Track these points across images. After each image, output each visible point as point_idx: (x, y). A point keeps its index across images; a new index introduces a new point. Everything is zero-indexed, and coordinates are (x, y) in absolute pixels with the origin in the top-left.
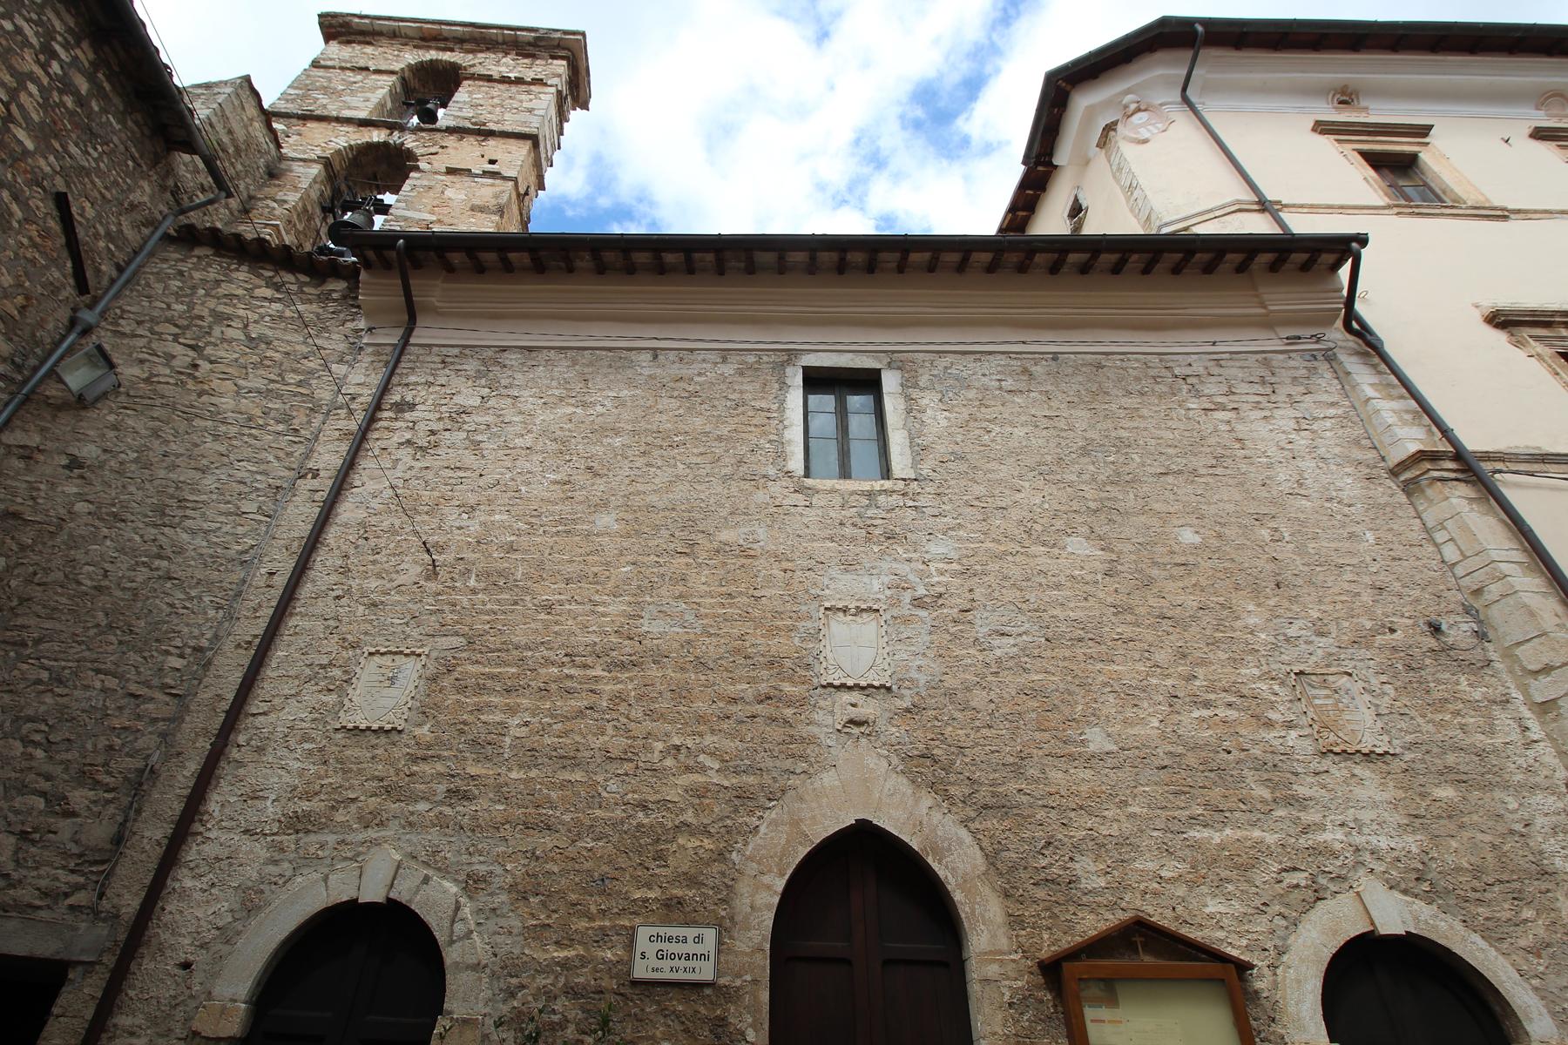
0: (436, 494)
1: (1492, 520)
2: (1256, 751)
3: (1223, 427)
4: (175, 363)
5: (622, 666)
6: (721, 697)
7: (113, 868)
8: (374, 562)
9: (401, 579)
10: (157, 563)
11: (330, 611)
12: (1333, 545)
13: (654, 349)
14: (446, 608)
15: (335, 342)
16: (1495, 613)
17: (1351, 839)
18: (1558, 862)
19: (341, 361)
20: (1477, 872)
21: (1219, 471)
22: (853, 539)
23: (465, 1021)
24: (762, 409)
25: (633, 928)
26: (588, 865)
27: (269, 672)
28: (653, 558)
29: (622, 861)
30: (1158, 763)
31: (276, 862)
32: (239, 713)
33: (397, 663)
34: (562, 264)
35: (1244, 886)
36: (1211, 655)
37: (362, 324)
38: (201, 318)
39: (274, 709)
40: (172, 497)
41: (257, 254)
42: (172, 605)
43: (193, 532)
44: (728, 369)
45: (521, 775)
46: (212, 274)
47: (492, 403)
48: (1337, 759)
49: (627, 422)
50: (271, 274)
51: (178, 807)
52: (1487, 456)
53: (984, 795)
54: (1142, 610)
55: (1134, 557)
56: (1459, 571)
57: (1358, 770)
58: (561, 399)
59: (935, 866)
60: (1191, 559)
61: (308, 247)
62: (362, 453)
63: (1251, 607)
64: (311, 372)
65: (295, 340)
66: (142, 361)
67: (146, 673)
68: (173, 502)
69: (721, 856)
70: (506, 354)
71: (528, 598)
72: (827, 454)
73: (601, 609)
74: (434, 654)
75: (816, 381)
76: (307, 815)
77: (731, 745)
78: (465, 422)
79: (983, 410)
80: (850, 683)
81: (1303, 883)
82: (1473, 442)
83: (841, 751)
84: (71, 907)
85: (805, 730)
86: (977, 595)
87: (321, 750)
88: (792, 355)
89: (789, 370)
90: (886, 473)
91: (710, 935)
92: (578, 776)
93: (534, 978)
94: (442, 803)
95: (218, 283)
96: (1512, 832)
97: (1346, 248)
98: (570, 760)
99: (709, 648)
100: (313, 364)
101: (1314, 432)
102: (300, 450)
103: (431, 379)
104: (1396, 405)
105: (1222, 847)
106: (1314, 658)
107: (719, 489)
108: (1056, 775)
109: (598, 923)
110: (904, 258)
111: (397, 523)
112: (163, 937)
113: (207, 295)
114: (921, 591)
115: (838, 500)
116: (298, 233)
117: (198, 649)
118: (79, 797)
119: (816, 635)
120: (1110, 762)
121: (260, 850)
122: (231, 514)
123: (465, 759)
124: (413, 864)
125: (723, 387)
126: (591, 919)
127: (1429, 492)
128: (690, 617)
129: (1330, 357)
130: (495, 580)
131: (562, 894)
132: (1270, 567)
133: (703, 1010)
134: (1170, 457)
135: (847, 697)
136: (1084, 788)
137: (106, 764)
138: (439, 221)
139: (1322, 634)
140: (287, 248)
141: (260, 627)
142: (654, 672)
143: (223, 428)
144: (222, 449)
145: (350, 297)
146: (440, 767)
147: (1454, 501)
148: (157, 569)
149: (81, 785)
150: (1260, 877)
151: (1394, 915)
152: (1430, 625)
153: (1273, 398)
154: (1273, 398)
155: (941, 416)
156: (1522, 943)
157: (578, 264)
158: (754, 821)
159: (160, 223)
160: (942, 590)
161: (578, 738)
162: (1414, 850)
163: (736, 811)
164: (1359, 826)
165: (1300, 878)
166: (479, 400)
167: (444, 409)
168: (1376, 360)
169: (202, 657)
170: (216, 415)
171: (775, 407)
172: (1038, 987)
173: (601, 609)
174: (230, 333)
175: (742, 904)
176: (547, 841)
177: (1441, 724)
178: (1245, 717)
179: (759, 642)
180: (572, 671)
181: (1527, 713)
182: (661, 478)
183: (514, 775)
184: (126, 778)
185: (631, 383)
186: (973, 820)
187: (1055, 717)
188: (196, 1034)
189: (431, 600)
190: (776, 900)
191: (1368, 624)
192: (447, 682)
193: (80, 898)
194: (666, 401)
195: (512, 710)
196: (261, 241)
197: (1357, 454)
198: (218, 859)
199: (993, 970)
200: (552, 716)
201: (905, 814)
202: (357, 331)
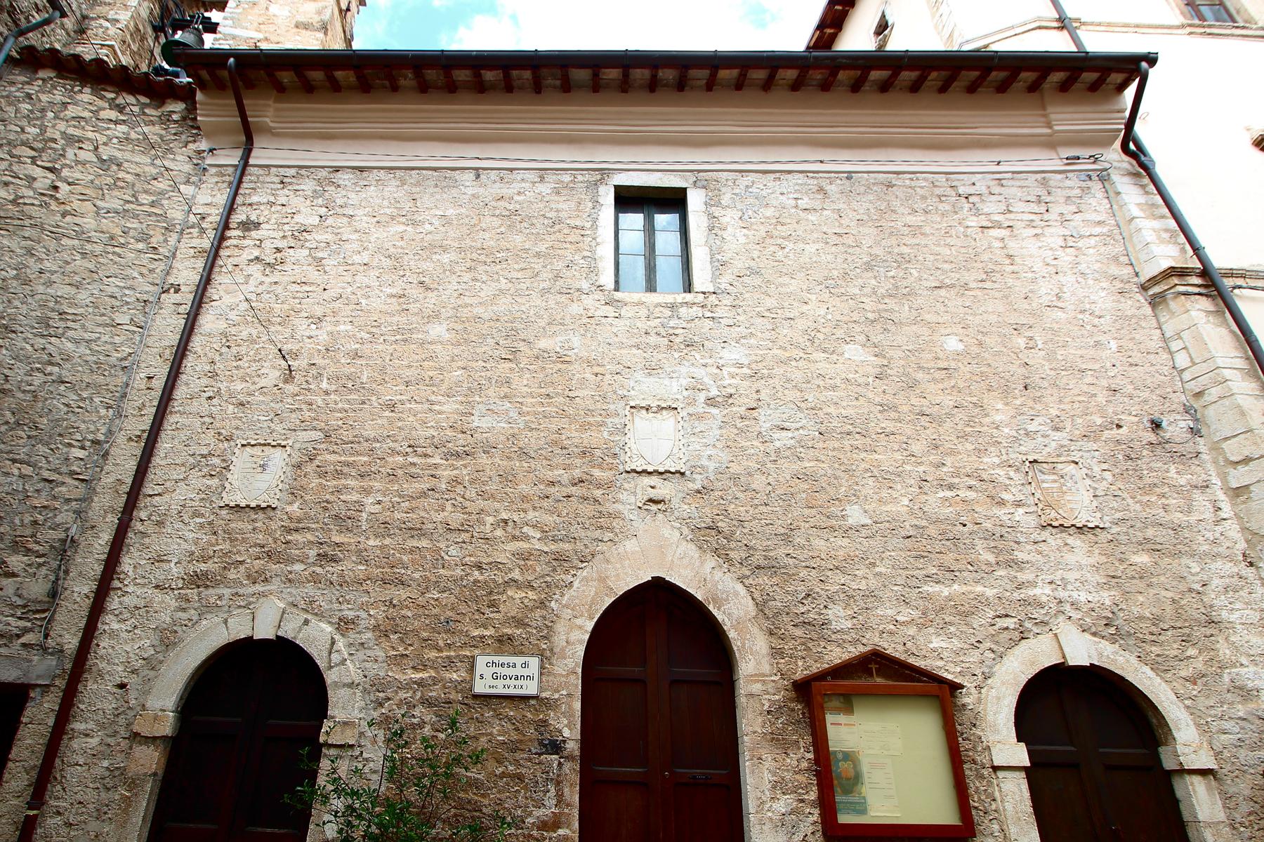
1: (1223, 331)
2: (988, 525)
3: (997, 244)
5: (458, 455)
7: (53, 616)
9: (263, 382)
10: (49, 369)
11: (205, 408)
12: (1079, 352)
13: (477, 169)
14: (303, 406)
15: (180, 163)
16: (1211, 413)
17: (1056, 594)
18: (1224, 614)
19: (188, 182)
20: (1156, 620)
21: (988, 285)
22: (656, 347)
23: (345, 723)
24: (576, 227)
25: (473, 657)
27: (156, 460)
29: (463, 608)
30: (904, 533)
32: (138, 494)
33: (266, 453)
34: (387, 83)
35: (964, 628)
37: (203, 145)
38: (54, 141)
39: (167, 491)
40: (53, 310)
42: (67, 405)
43: (76, 342)
44: (545, 189)
45: (378, 543)
46: (58, 96)
47: (330, 221)
48: (1054, 531)
49: (454, 239)
50: (113, 95)
51: (99, 569)
52: (1231, 274)
53: (758, 559)
54: (905, 409)
56: (1187, 376)
57: (1070, 540)
59: (715, 612)
60: (953, 365)
61: (144, 68)
62: (216, 269)
64: (162, 193)
66: (6, 184)
67: (55, 461)
68: (55, 315)
70: (339, 175)
71: (374, 398)
72: (635, 269)
74: (297, 446)
75: (628, 199)
76: (205, 574)
77: (550, 519)
78: (306, 240)
79: (779, 227)
80: (650, 469)
81: (1012, 626)
82: (1219, 259)
83: (640, 523)
85: (612, 508)
86: (763, 396)
87: (210, 523)
89: (602, 189)
90: (688, 287)
92: (424, 543)
93: (397, 692)
95: (65, 105)
96: (1190, 590)
97: (1133, 68)
98: (418, 531)
99: (531, 441)
100: (162, 185)
101: (1078, 249)
102: (160, 267)
103: (272, 199)
104: (1157, 224)
105: (949, 598)
107: (538, 302)
108: (819, 543)
109: (445, 654)
110: (713, 76)
111: (254, 333)
112: (101, 666)
114: (714, 392)
115: (643, 312)
116: (133, 53)
117: (96, 442)
119: (622, 430)
120: (864, 533)
121: (170, 601)
122: (107, 325)
123: (330, 530)
124: (294, 610)
125: (541, 205)
127: (1173, 305)
129: (1104, 177)
131: (416, 632)
132: (1022, 371)
134: (945, 272)
135: (647, 481)
138: (266, 39)
140: (125, 68)
141: (146, 423)
142: (484, 460)
144: (91, 266)
145: (189, 119)
146: (309, 537)
147: (1193, 313)
148: (50, 374)
149: (16, 552)
151: (1082, 651)
152: (1153, 422)
153: (1046, 217)
154: (1046, 217)
155: (740, 234)
156: (1183, 673)
157: (402, 82)
160: (733, 391)
161: (423, 514)
162: (1108, 602)
164: (1065, 583)
166: (318, 219)
167: (286, 227)
168: (1147, 180)
169: (100, 448)
170: (80, 234)
171: (588, 225)
173: (437, 407)
174: (83, 155)
177: (1148, 504)
178: (982, 498)
179: (574, 436)
180: (415, 460)
181: (1221, 496)
184: (52, 547)
185: (456, 202)
186: (748, 577)
187: (821, 498)
188: (137, 734)
191: (1099, 421)
192: (309, 468)
194: (488, 219)
195: (367, 491)
196: (99, 62)
197: (1114, 270)
200: (400, 496)
201: (692, 572)
202: (199, 152)
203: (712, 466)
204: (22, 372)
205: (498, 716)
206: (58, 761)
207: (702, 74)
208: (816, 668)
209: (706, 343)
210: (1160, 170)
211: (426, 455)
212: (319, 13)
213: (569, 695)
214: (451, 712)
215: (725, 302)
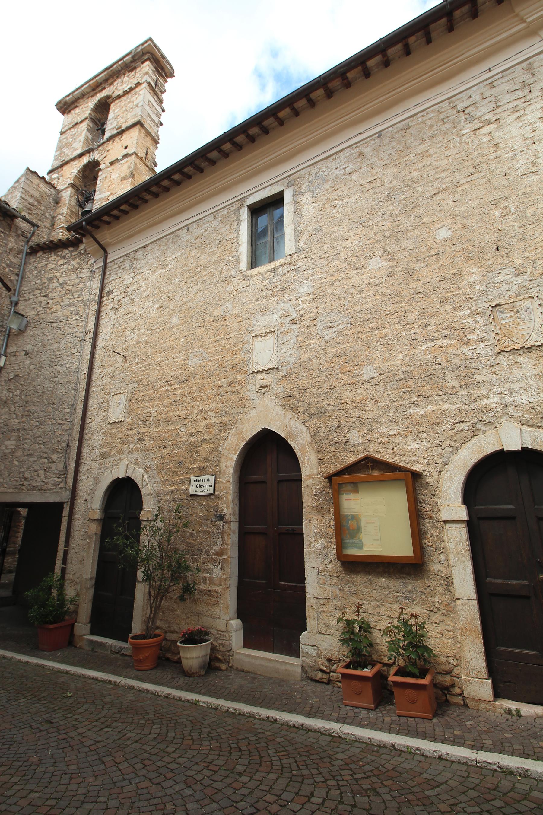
0: (123, 327)
2: (456, 361)
4: (43, 304)
6: (215, 387)
8: (110, 361)
26: (177, 458)
27: (90, 408)
28: (192, 332)
30: (398, 378)
31: (100, 469)
35: (432, 434)
36: (441, 309)
41: (53, 247)
42: (62, 393)
43: (62, 366)
48: (507, 355)
53: (313, 410)
55: (407, 259)
57: (520, 359)
58: (157, 267)
63: (475, 270)
65: (72, 279)
68: (54, 357)
69: (216, 449)
73: (175, 360)
77: (219, 406)
81: (466, 428)
84: (60, 488)
85: (244, 394)
88: (243, 200)
91: (212, 478)
92: (172, 427)
94: (136, 443)
98: (169, 422)
99: (211, 367)
106: (510, 293)
113: (45, 272)
117: (72, 405)
118: (54, 457)
120: (373, 383)
123: (141, 427)
126: (179, 476)
128: (204, 355)
130: (144, 357)
133: (211, 503)
135: (260, 376)
136: (359, 398)
137: (58, 446)
139: (520, 275)
143: (61, 324)
150: (440, 429)
158: (227, 435)
159: (23, 250)
163: (221, 432)
165: (465, 426)
172: (327, 487)
175: (223, 466)
176: (165, 452)
182: (193, 291)
183: (154, 430)
186: (308, 421)
189: (126, 371)
190: (234, 463)
193: (62, 485)
198: (88, 470)
199: (310, 482)
200: (164, 407)
201: (281, 423)
203: (291, 360)
204: (47, 383)
207: (320, 92)
211: (172, 385)
212: (129, 168)
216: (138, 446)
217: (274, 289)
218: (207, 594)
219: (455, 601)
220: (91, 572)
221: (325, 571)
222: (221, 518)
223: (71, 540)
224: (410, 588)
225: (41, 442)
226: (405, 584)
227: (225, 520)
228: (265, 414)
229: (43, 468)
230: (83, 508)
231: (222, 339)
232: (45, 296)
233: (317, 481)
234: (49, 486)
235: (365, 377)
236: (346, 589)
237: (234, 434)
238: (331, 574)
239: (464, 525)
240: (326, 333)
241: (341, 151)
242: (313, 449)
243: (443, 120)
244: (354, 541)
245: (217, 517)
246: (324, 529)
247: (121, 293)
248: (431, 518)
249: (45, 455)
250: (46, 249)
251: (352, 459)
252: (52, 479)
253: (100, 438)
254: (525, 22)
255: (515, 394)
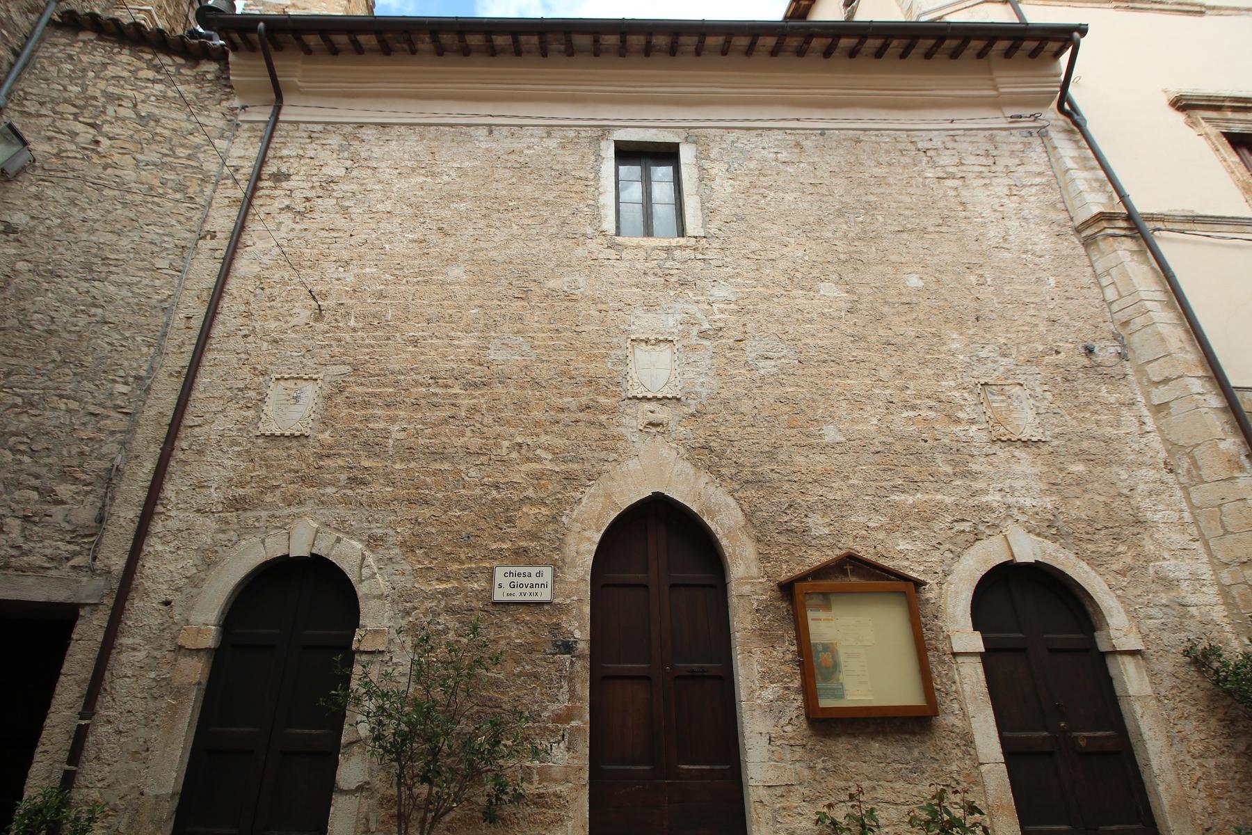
0: (316, 251)
1: (1145, 268)
2: (946, 441)
3: (952, 193)
4: (79, 139)
5: (476, 385)
6: (552, 408)
7: (100, 540)
8: (271, 308)
9: (294, 321)
10: (93, 310)
11: (240, 344)
12: (1023, 288)
13: (489, 125)
14: (333, 343)
15: (214, 119)
16: (1136, 340)
17: (1005, 500)
18: (1149, 515)
19: (222, 137)
20: (1091, 521)
21: (944, 229)
22: (654, 286)
23: (376, 631)
24: (581, 178)
25: (492, 568)
26: (457, 528)
27: (196, 394)
29: (482, 524)
30: (873, 449)
31: (224, 531)
32: (179, 426)
33: (299, 386)
34: (406, 46)
35: (926, 532)
37: (236, 103)
38: (95, 98)
39: (206, 422)
40: (96, 256)
42: (111, 344)
44: (552, 143)
45: (403, 466)
46: (99, 57)
47: (355, 173)
48: (1003, 445)
49: (469, 190)
50: (150, 57)
51: (143, 495)
52: (1151, 218)
53: (746, 474)
54: (873, 339)
56: (1115, 307)
57: (1017, 453)
58: (413, 170)
59: (709, 523)
60: (914, 299)
61: (180, 31)
62: (250, 217)
63: (955, 336)
64: (198, 147)
65: (176, 118)
66: (50, 139)
67: (100, 397)
70: (363, 130)
71: (398, 335)
72: (633, 214)
73: (456, 342)
74: (328, 379)
75: (627, 153)
76: (243, 498)
78: (333, 190)
79: (761, 178)
80: (650, 396)
81: (968, 529)
82: (1142, 206)
83: (643, 445)
86: (748, 329)
87: (247, 451)
88: (606, 130)
89: (603, 144)
90: (682, 232)
91: (548, 571)
93: (423, 602)
95: (105, 65)
96: (1120, 495)
97: (1067, 37)
98: (441, 456)
99: (543, 372)
100: (198, 139)
101: (1021, 197)
102: (197, 215)
103: (301, 152)
104: (1087, 175)
105: (913, 506)
106: (997, 373)
107: (547, 246)
108: (800, 460)
109: (466, 566)
110: (702, 42)
111: (286, 275)
112: (146, 585)
113: (97, 77)
114: (706, 326)
115: (642, 255)
116: (169, 18)
118: (65, 490)
119: (624, 361)
120: (839, 449)
121: (211, 523)
122: (148, 269)
123: (359, 456)
124: (327, 529)
125: (548, 159)
126: (462, 563)
127: (1102, 245)
128: (526, 348)
129: (1042, 133)
130: (372, 322)
131: (440, 547)
132: (974, 304)
133: (544, 619)
134: (907, 217)
135: (648, 406)
136: (819, 467)
137: (80, 466)
138: (294, 6)
139: (1004, 355)
140: (161, 32)
141: (185, 360)
142: (499, 389)
143: (129, 197)
144: (132, 215)
145: (223, 81)
146: (340, 462)
147: (1120, 253)
148: (94, 315)
149: (64, 481)
150: (937, 525)
151: (1027, 550)
152: (1086, 348)
153: (993, 169)
154: (993, 169)
155: (727, 184)
156: (1115, 567)
157: (420, 46)
158: (578, 495)
160: (722, 325)
161: (444, 439)
162: (1049, 507)
163: (565, 488)
164: (1013, 490)
165: (966, 526)
166: (344, 171)
167: (315, 178)
168: (1079, 136)
169: (143, 384)
170: (121, 185)
171: (591, 176)
172: (777, 599)
173: (456, 342)
174: (123, 112)
175: (570, 551)
177: (1083, 420)
178: (940, 416)
179: (581, 367)
180: (437, 390)
181: (1145, 412)
182: (500, 236)
183: (398, 466)
184: (98, 476)
185: (471, 156)
186: (737, 491)
187: (801, 419)
188: (181, 647)
189: (320, 337)
190: (595, 547)
191: (1041, 348)
192: (339, 399)
194: (501, 171)
195: (393, 420)
196: (137, 26)
197: (1053, 215)
198: (180, 531)
199: (746, 589)
200: (423, 424)
201: (688, 487)
202: (232, 109)
203: (704, 392)
204: (67, 314)
205: (515, 621)
206: (107, 674)
208: (798, 570)
209: (698, 282)
210: (1091, 128)
211: (446, 386)
213: (580, 600)
214: (473, 618)
215: (714, 245)
216: (349, 492)
217: (668, 278)
218: (535, 803)
219: (977, 768)
220: (176, 779)
221: (782, 738)
222: (568, 647)
223: (104, 700)
224: (916, 754)
225: (22, 447)
226: (910, 749)
227: (577, 653)
228: (652, 468)
229: (22, 513)
230: (155, 621)
231: (565, 329)
232: (92, 126)
233: (758, 588)
234: (36, 560)
235: (827, 439)
236: (820, 766)
237: (593, 496)
238: (792, 742)
239: (979, 659)
240: (760, 365)
241: (770, 129)
242: (750, 537)
243: (901, 151)
244: (830, 685)
245: (558, 646)
246: (775, 666)
247: (313, 187)
248: (937, 649)
249: (37, 483)
250: (110, 34)
251: (816, 559)
252: (47, 543)
253: (229, 463)
254: (997, 90)
255: (1017, 494)
